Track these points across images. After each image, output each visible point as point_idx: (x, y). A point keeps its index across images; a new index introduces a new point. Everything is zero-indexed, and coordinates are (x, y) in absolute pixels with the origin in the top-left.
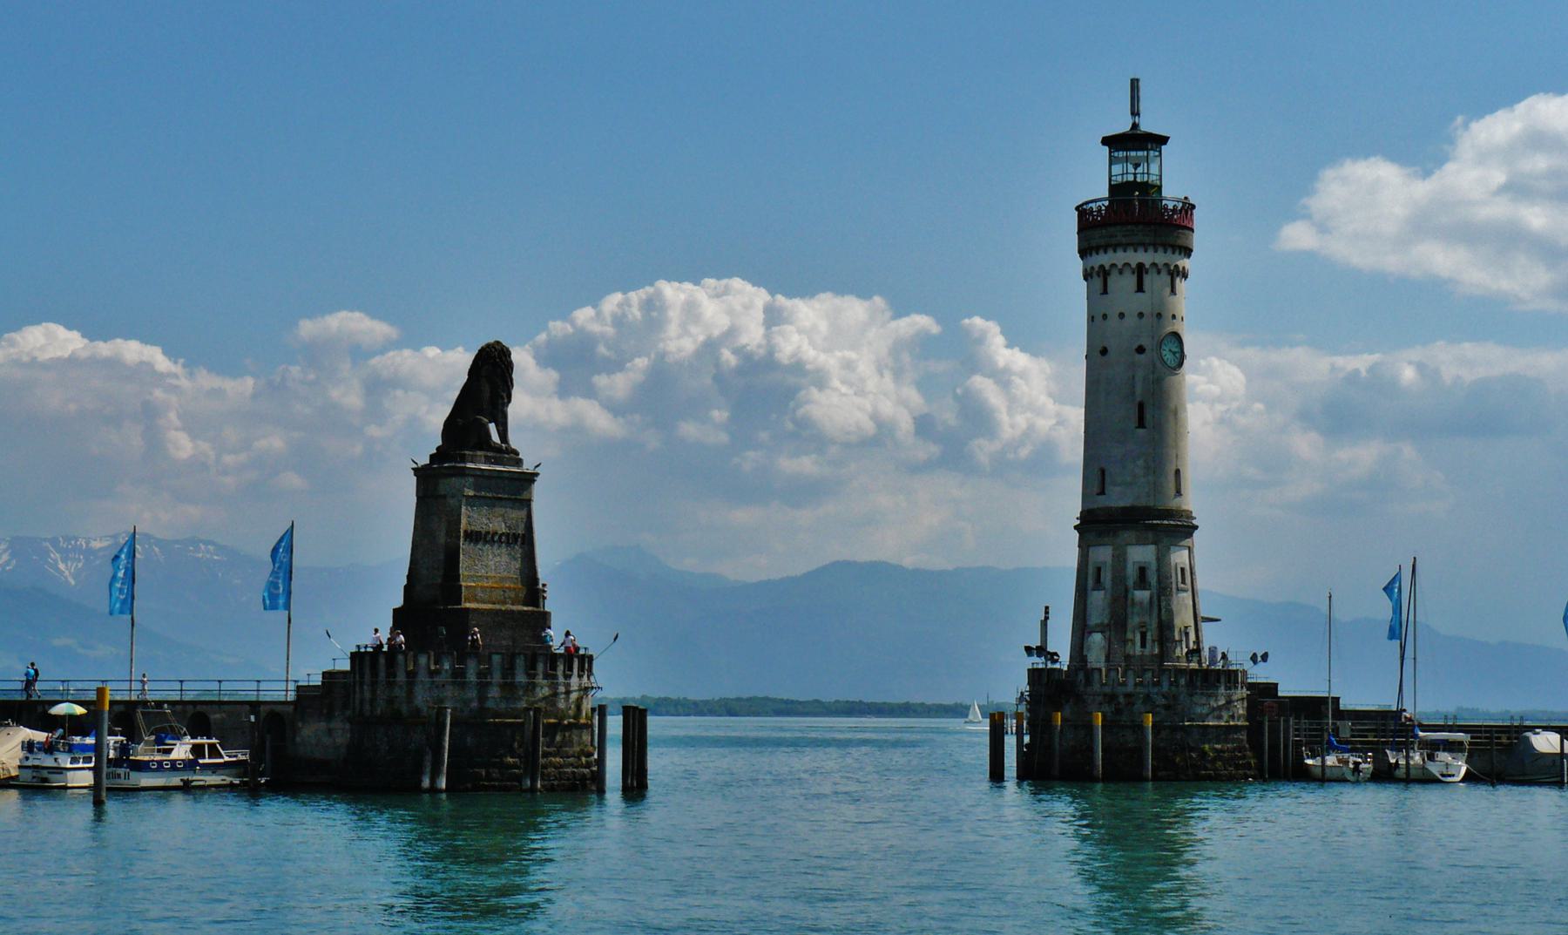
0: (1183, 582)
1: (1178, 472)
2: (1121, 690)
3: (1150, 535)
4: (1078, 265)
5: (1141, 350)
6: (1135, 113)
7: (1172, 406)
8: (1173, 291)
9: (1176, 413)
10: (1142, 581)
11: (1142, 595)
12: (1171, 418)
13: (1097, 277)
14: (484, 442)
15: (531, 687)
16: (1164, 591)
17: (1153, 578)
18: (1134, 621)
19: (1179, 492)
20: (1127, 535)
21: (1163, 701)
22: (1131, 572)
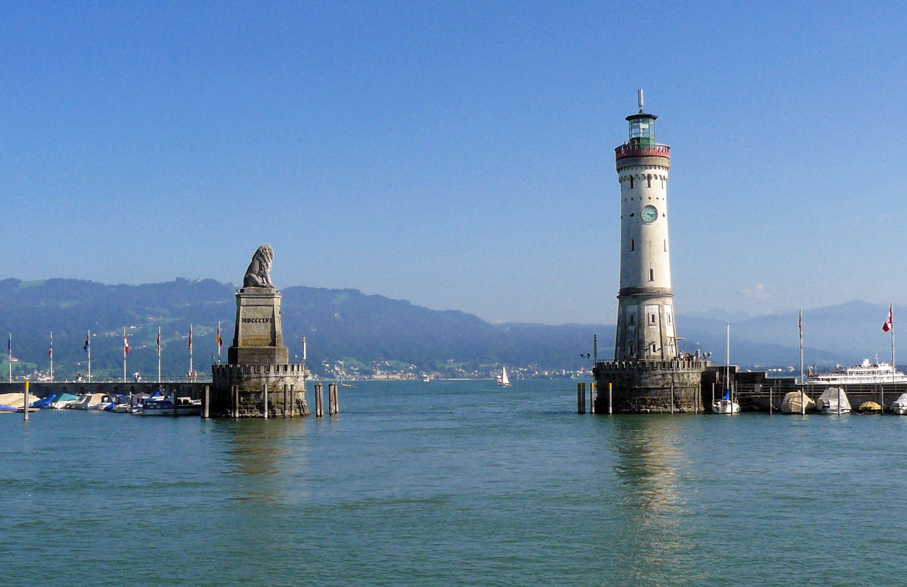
0: (653, 321)
1: (651, 271)
2: (611, 372)
3: (635, 300)
4: (617, 176)
5: (632, 215)
6: (640, 106)
7: (648, 240)
8: (649, 186)
9: (650, 242)
10: (632, 323)
11: (632, 328)
12: (647, 246)
13: (620, 181)
14: (256, 284)
15: (249, 379)
16: (640, 326)
17: (636, 320)
18: (628, 340)
19: (652, 279)
20: (626, 301)
21: (627, 377)
22: (628, 320)
